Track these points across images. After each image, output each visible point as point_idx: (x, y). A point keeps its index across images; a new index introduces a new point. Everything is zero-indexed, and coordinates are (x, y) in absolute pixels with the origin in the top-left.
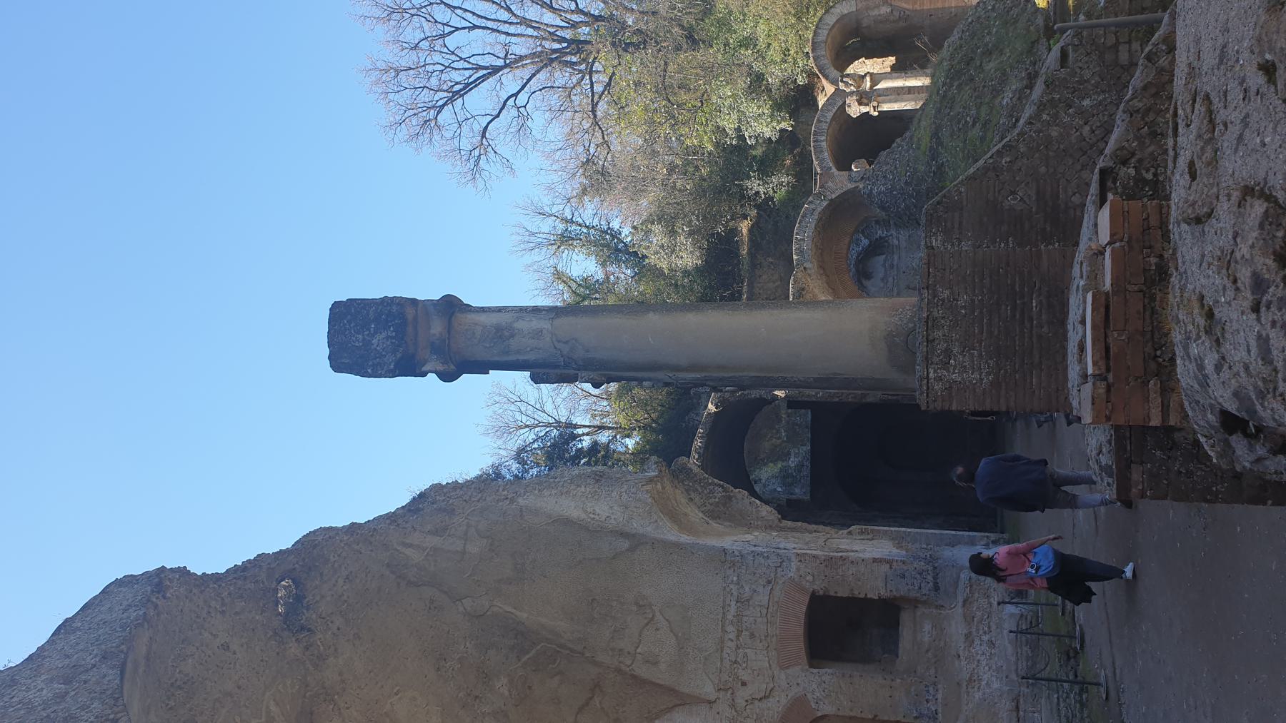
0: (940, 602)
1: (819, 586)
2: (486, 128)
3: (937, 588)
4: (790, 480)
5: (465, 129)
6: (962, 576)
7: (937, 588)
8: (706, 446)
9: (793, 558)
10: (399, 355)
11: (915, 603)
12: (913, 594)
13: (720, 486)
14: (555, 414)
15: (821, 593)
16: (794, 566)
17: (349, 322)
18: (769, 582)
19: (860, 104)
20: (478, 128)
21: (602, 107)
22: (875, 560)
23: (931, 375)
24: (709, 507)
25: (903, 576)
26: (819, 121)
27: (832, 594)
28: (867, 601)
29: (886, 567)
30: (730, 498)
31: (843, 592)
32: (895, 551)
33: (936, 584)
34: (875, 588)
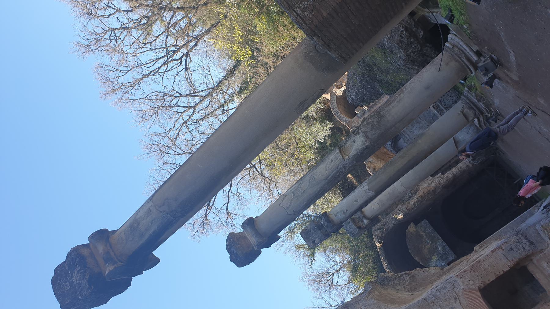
0: (540, 248)
1: (479, 283)
2: (227, 208)
3: (532, 243)
4: (444, 257)
5: (221, 215)
6: (537, 228)
7: (532, 243)
8: (390, 263)
9: (457, 279)
10: (87, 277)
11: (528, 258)
12: (524, 254)
13: (405, 274)
14: (336, 304)
15: (482, 286)
16: (460, 282)
17: (60, 280)
18: (456, 299)
19: (339, 88)
20: (225, 211)
21: (267, 174)
22: (493, 252)
23: (299, 11)
24: (408, 287)
25: (512, 249)
26: (333, 109)
27: (488, 282)
28: (506, 274)
29: (500, 252)
30: (413, 276)
31: (492, 278)
32: (499, 242)
33: (529, 241)
34: (504, 265)
